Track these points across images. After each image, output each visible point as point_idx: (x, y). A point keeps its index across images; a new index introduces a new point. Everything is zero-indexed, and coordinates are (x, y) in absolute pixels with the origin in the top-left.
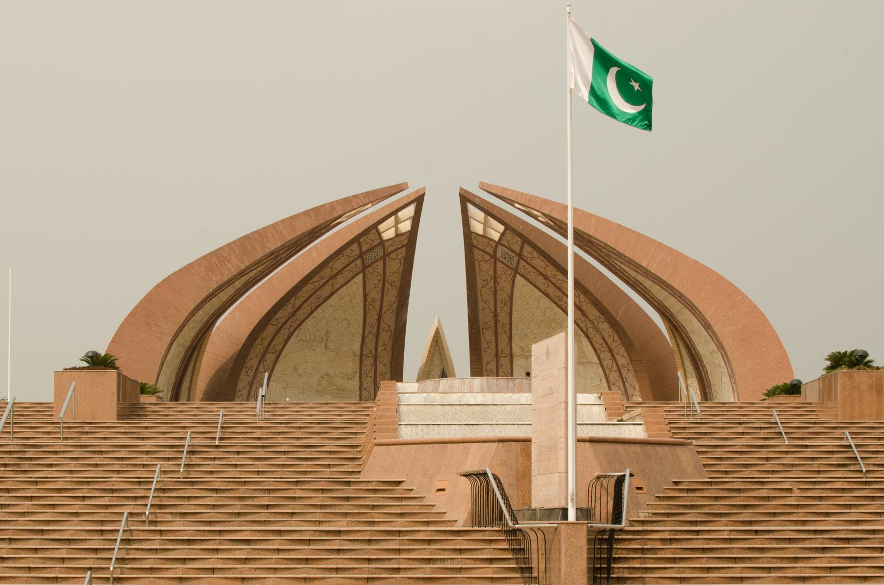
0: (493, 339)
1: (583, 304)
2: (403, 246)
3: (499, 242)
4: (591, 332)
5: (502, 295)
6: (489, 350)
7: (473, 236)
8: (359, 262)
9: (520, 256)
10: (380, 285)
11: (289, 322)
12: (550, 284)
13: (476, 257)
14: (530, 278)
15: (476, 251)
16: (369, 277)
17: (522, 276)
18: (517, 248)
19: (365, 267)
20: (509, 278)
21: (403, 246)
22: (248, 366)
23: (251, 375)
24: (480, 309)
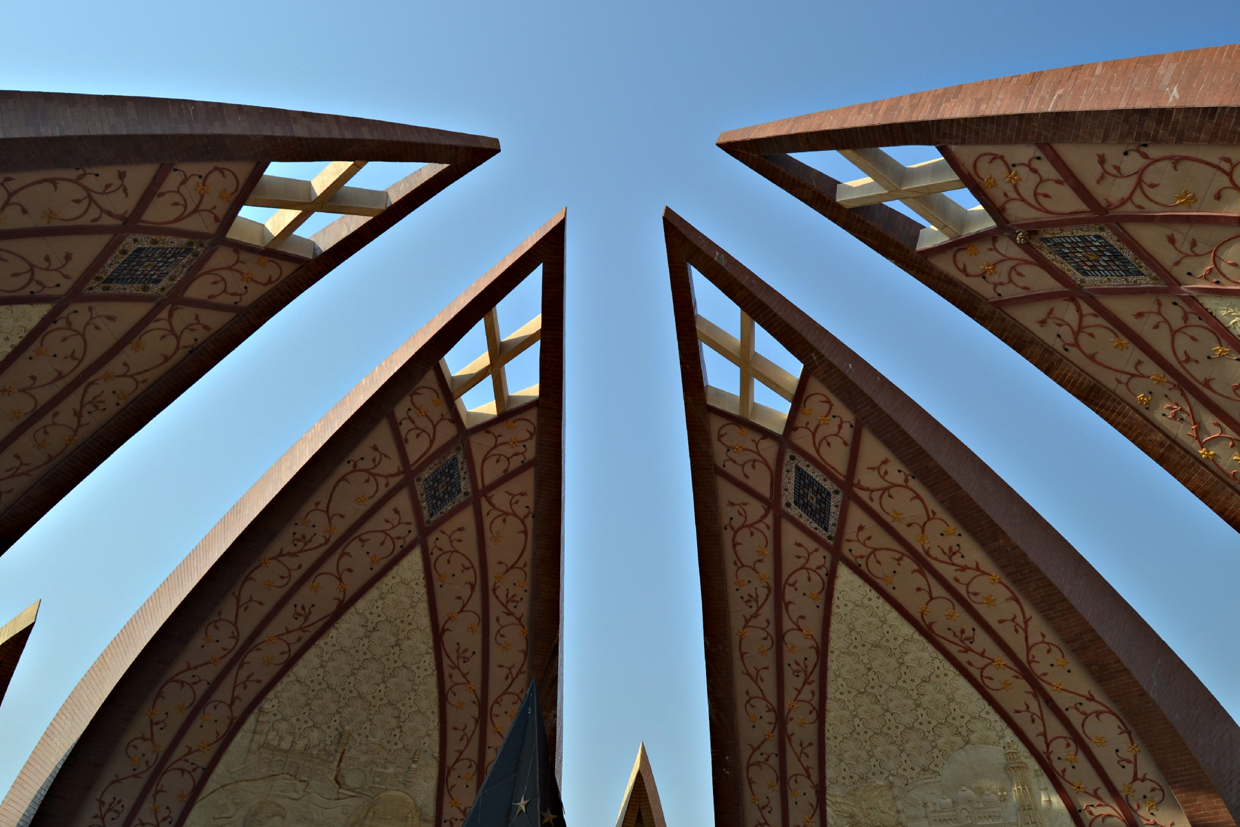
0: (775, 796)
1: (1039, 652)
3: (785, 440)
4: (1062, 751)
5: (799, 646)
7: (716, 423)
8: (402, 501)
9: (848, 485)
10: (476, 604)
12: (938, 590)
13: (727, 514)
14: (875, 570)
15: (727, 492)
16: (441, 566)
17: (856, 569)
18: (837, 457)
19: (425, 530)
20: (817, 583)
22: (108, 799)
24: (741, 699)
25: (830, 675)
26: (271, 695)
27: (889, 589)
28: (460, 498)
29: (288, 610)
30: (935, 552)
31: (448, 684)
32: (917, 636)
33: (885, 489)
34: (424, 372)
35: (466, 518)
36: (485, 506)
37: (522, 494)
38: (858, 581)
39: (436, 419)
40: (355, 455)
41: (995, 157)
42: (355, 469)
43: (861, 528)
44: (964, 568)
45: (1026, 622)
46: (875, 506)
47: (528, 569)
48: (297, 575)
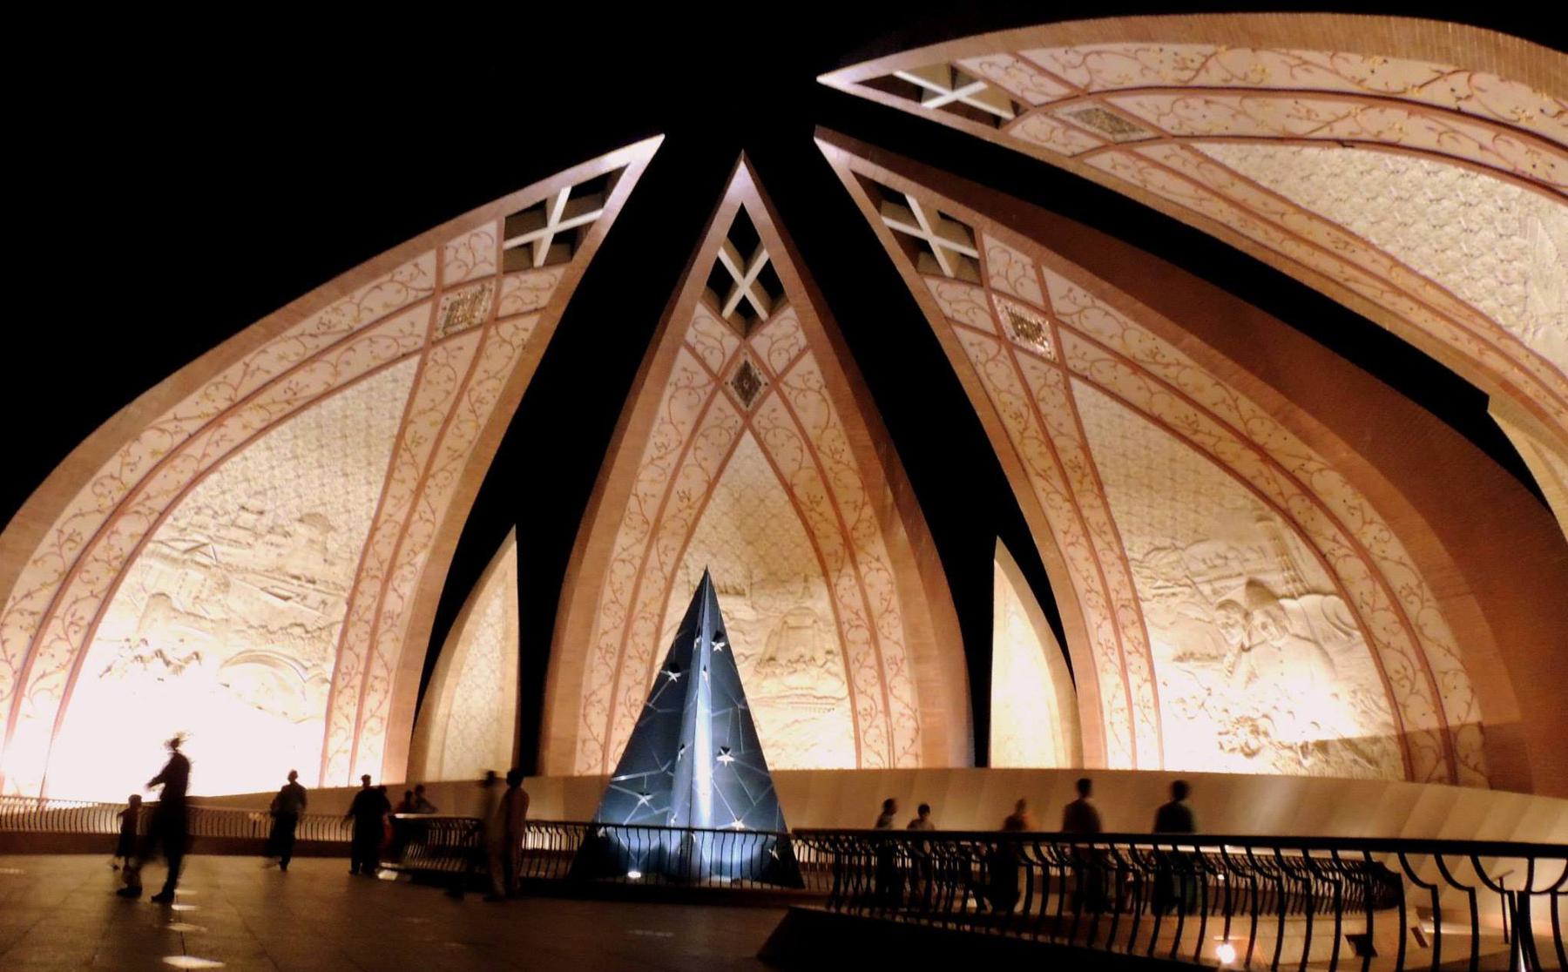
1: (1255, 425)
2: (802, 353)
4: (1298, 505)
6: (1093, 596)
8: (720, 399)
11: (654, 553)
12: (1154, 386)
13: (973, 352)
15: (965, 336)
16: (770, 439)
17: (1085, 379)
18: (1032, 293)
19: (747, 417)
21: (802, 353)
22: (603, 644)
23: (613, 663)
24: (1042, 496)
25: (1100, 468)
26: (686, 556)
27: (1116, 390)
28: (762, 389)
29: (674, 496)
30: (1140, 356)
31: (811, 523)
32: (1151, 426)
33: (1080, 312)
34: (693, 308)
35: (774, 398)
36: (786, 390)
37: (811, 373)
38: (1090, 390)
39: (718, 336)
40: (673, 378)
41: (990, 65)
42: (677, 389)
43: (1075, 347)
44: (1167, 365)
45: (1235, 401)
46: (1077, 326)
47: (840, 426)
48: (669, 472)
